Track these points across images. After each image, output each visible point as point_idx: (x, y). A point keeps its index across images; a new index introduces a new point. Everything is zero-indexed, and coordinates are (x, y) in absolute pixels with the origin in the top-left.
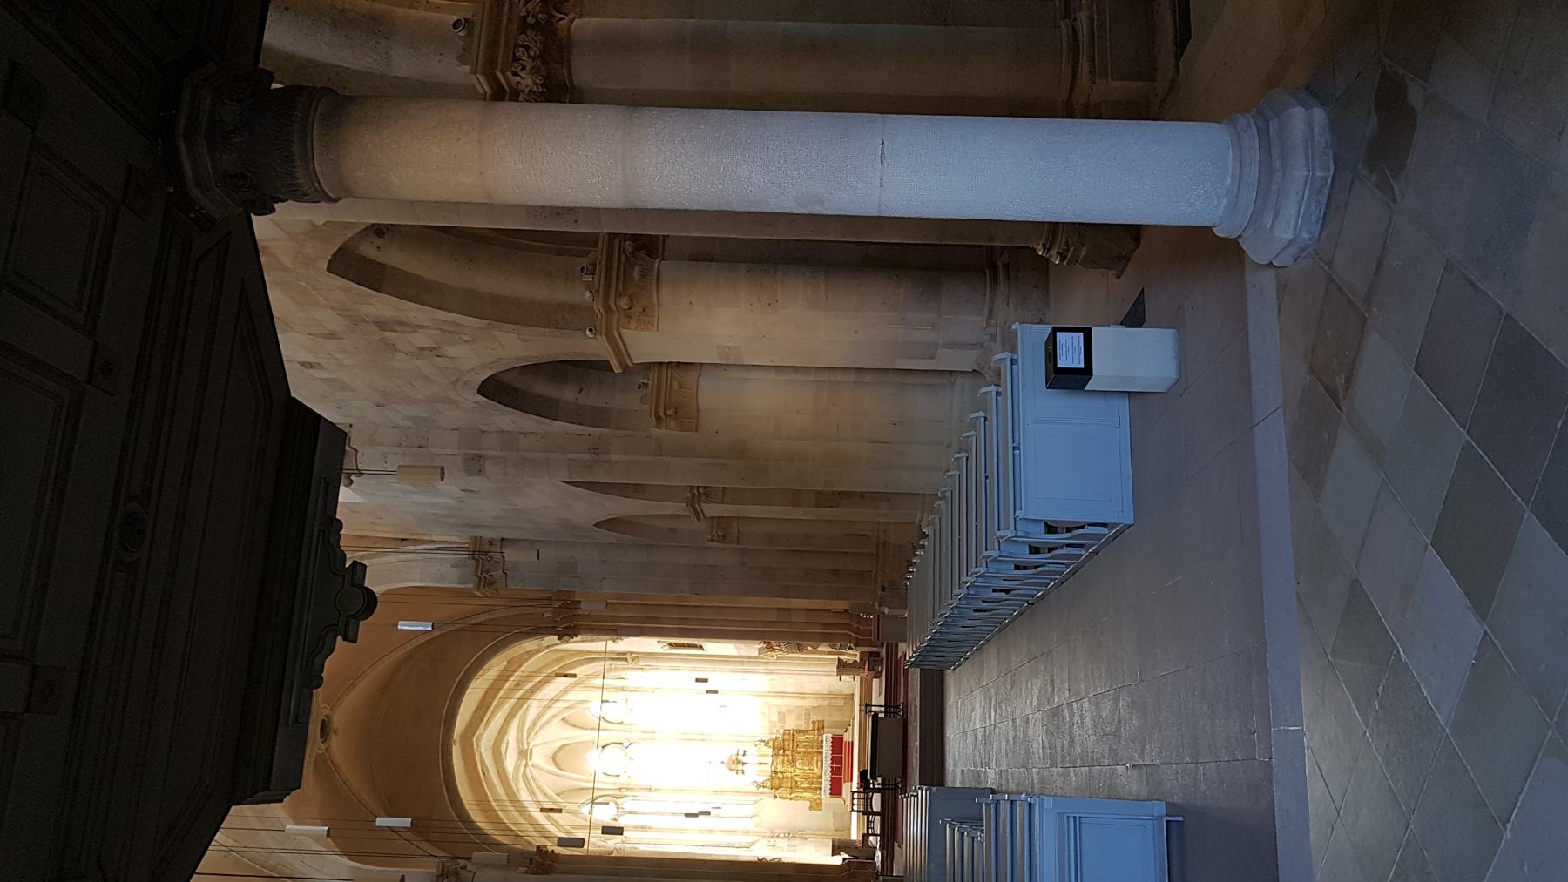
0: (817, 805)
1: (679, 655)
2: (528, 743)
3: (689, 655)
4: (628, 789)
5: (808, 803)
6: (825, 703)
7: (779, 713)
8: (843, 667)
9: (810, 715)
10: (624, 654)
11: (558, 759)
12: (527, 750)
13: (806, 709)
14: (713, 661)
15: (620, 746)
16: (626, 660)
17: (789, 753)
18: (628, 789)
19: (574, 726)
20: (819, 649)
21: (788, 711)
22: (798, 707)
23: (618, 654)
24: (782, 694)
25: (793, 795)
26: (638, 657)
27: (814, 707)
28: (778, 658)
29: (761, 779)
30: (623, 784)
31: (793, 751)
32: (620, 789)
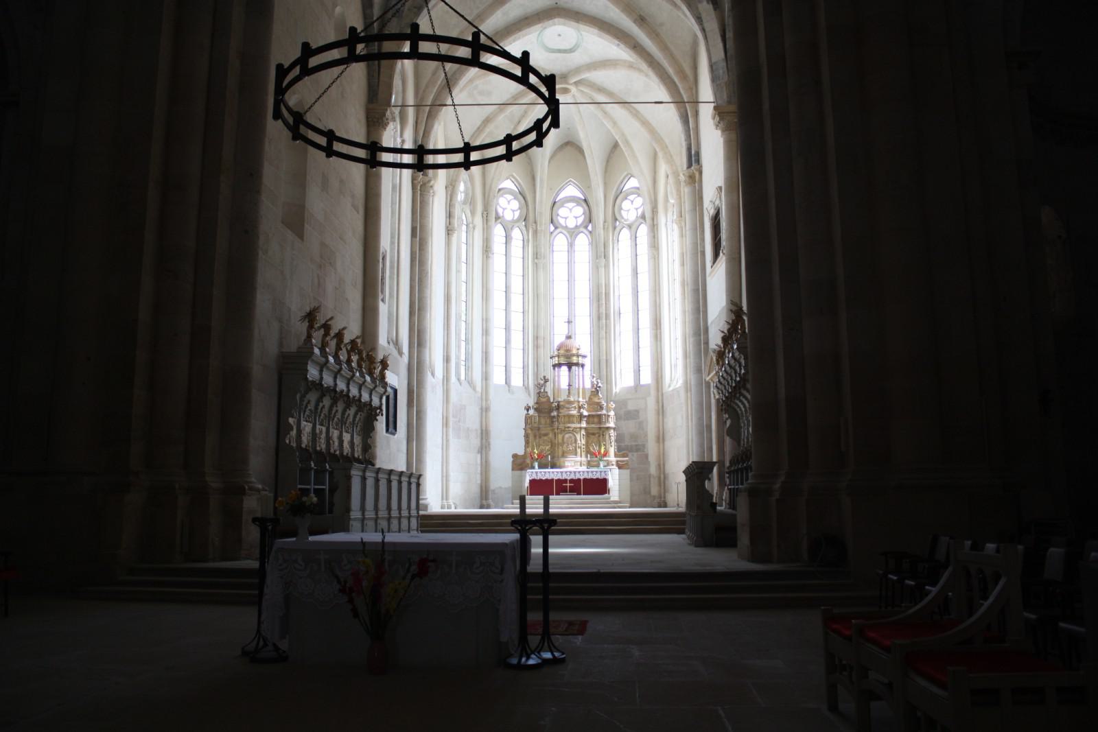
0: (520, 464)
1: (703, 240)
2: (576, 83)
3: (703, 253)
4: (535, 232)
5: (521, 452)
6: (653, 470)
7: (637, 411)
8: (697, 473)
9: (637, 450)
10: (698, 161)
11: (569, 148)
12: (568, 84)
13: (644, 446)
14: (698, 290)
15: (587, 220)
16: (690, 165)
17: (584, 425)
18: (535, 232)
19: (608, 161)
20: (728, 440)
21: (641, 423)
22: (646, 435)
23: (698, 154)
24: (661, 411)
25: (529, 432)
26: (695, 184)
27: (647, 456)
28: (708, 384)
29: (549, 388)
30: (540, 225)
31: (585, 429)
32: (535, 222)
